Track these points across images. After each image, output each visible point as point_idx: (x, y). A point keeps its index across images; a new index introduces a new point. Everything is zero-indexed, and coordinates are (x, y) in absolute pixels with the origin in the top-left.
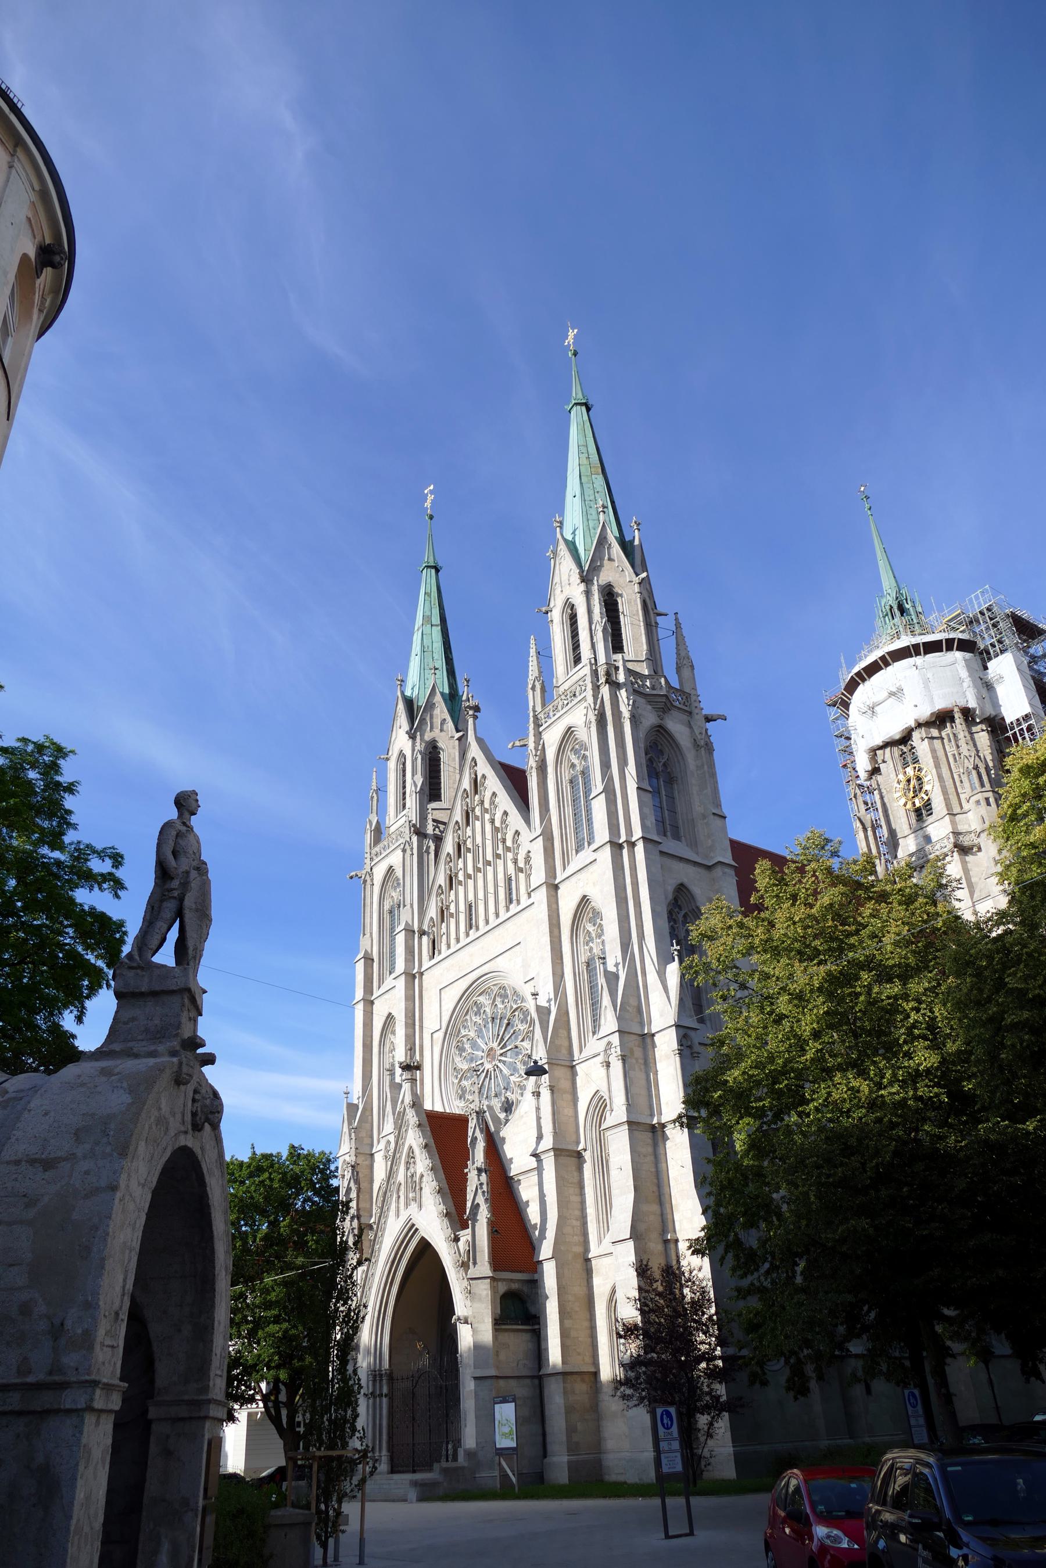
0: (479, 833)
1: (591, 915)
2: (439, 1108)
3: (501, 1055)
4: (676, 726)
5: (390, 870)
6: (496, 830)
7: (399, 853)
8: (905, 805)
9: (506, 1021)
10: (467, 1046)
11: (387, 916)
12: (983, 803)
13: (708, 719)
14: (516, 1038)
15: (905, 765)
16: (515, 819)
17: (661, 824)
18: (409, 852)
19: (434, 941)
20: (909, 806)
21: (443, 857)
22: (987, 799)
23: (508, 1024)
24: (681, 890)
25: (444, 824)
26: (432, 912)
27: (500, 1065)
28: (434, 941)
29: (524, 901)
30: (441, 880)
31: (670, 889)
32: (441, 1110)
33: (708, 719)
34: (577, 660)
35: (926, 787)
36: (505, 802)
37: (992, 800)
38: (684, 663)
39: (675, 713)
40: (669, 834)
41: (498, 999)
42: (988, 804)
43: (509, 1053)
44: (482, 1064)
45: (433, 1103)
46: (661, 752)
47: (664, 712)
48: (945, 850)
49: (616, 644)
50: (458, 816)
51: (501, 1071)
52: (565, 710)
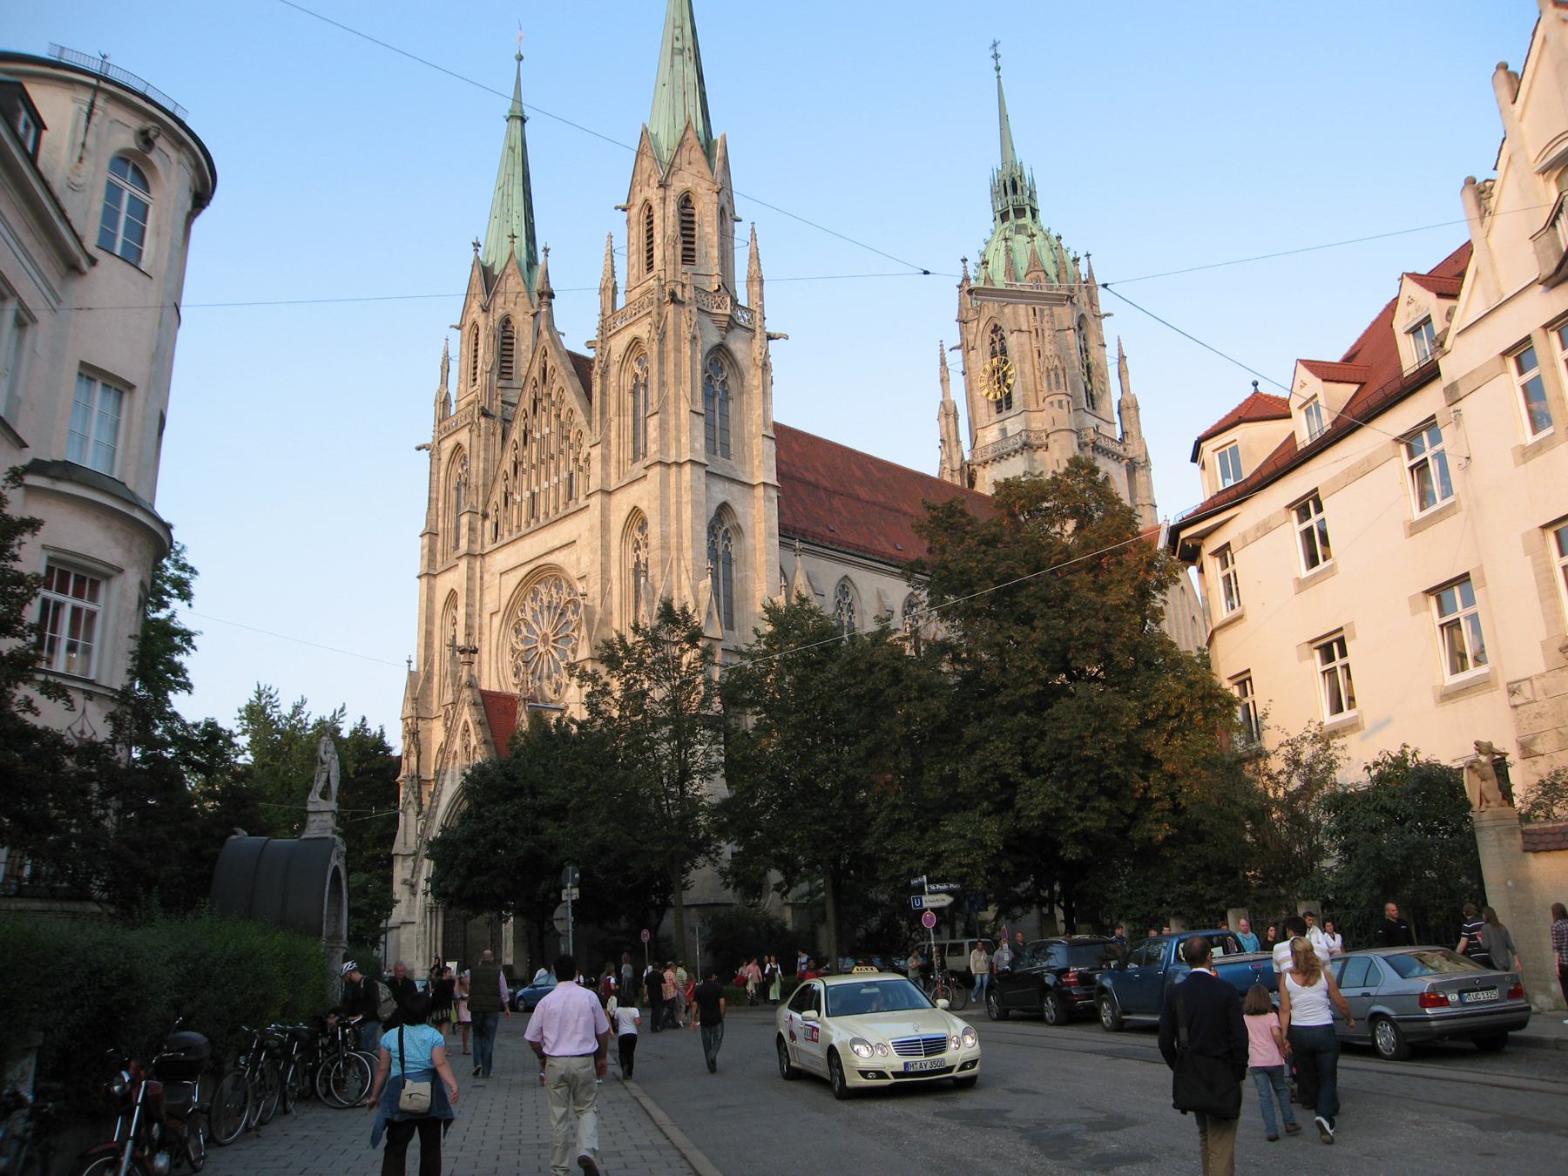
0: (545, 427)
1: (640, 524)
2: (495, 688)
3: (554, 641)
4: (737, 346)
5: (458, 446)
6: (562, 426)
7: (466, 430)
8: (988, 394)
9: (559, 611)
10: (524, 630)
11: (454, 493)
12: (1056, 404)
13: (770, 337)
14: (568, 628)
15: (994, 355)
16: (579, 418)
17: (712, 443)
18: (476, 432)
19: (497, 525)
20: (991, 397)
21: (510, 442)
22: (1060, 401)
23: (561, 614)
24: (724, 508)
25: (513, 405)
26: (498, 497)
27: (552, 651)
28: (497, 525)
29: (582, 502)
30: (508, 466)
31: (714, 507)
32: (498, 690)
33: (770, 337)
34: (650, 267)
35: (1010, 381)
36: (572, 399)
37: (1065, 403)
38: (756, 280)
39: (738, 331)
40: (719, 452)
41: (553, 589)
42: (1061, 406)
43: (560, 641)
44: (536, 647)
45: (489, 683)
46: (721, 369)
47: (727, 331)
48: (1017, 447)
49: (688, 256)
50: (526, 404)
51: (553, 656)
52: (632, 320)
